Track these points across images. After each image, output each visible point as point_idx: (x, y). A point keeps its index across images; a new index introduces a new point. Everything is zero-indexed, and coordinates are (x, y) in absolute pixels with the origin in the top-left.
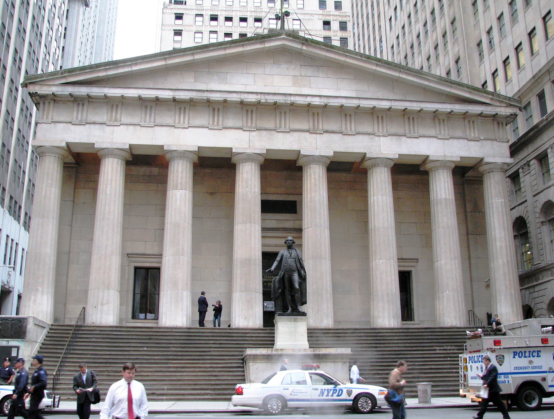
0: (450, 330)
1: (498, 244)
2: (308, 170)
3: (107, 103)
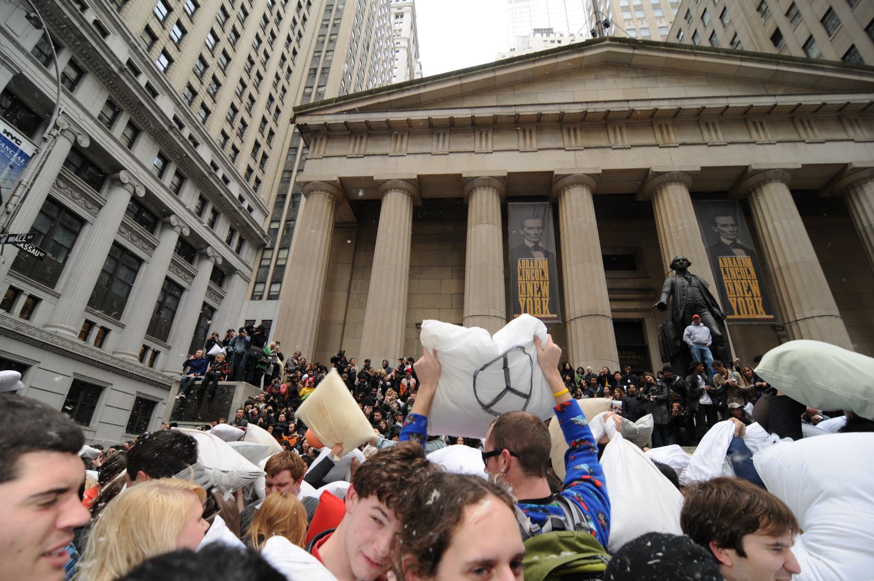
2: (664, 193)
3: (390, 135)
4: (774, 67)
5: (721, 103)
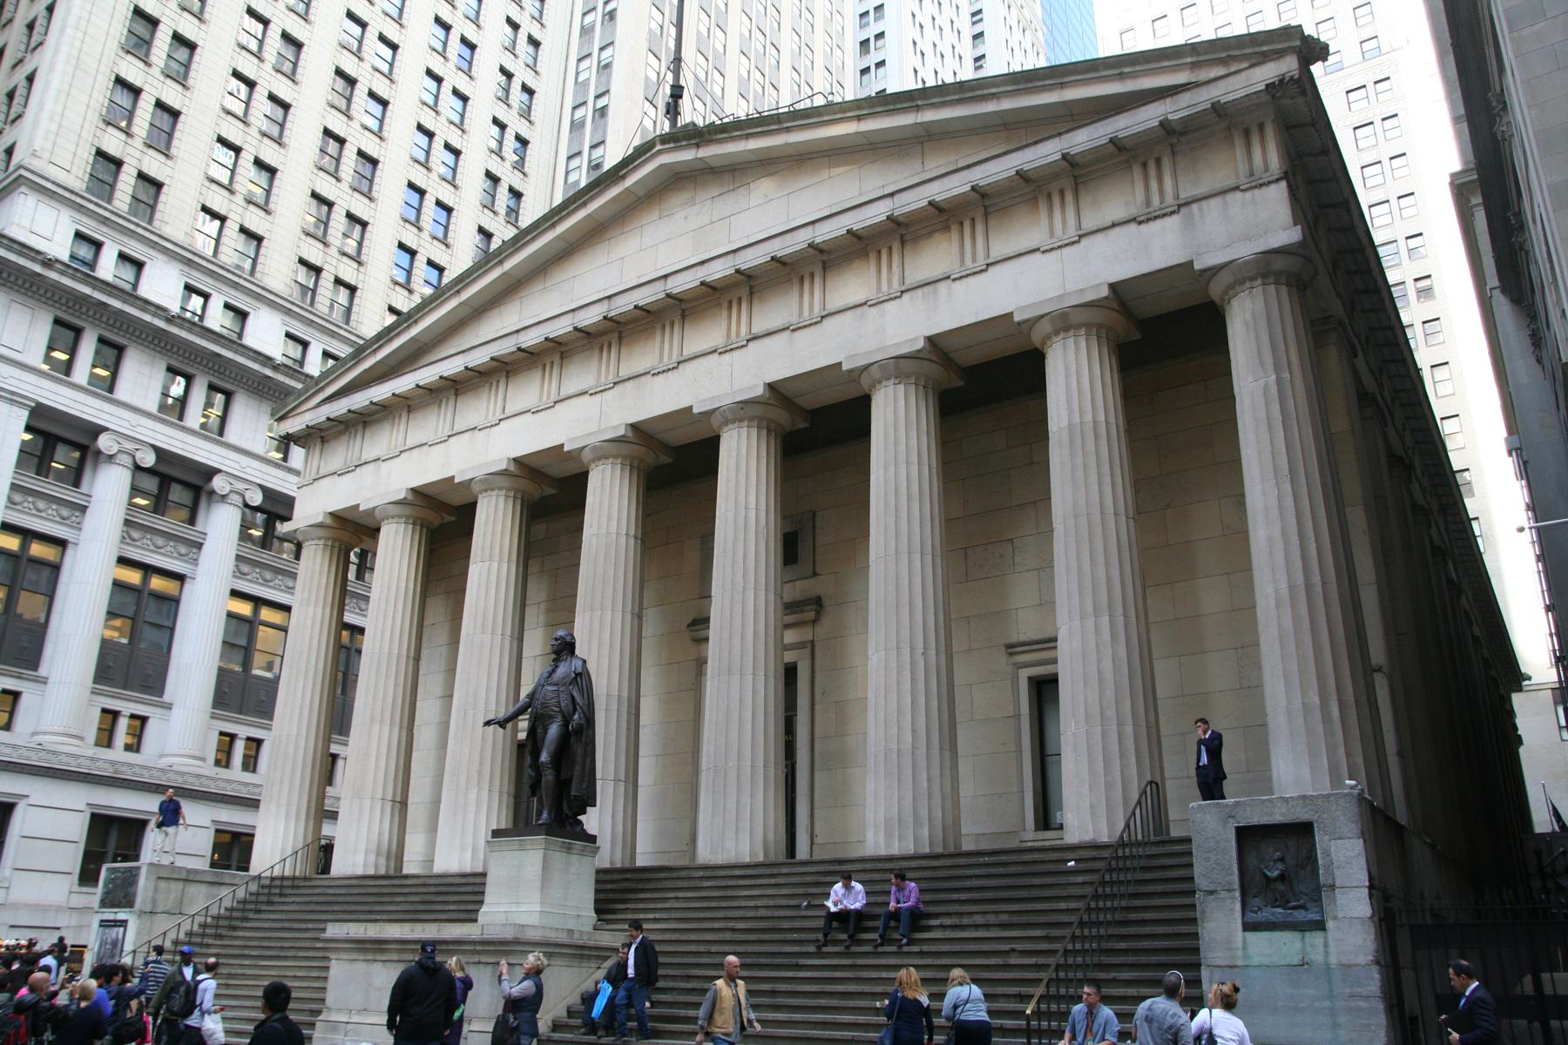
0: (1014, 858)
5: (798, 242)
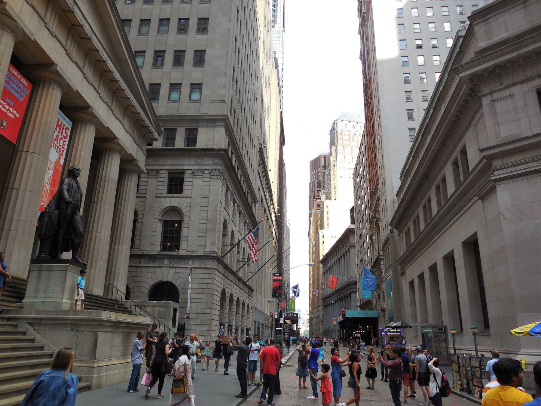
1: (126, 231)
4: (127, 58)
